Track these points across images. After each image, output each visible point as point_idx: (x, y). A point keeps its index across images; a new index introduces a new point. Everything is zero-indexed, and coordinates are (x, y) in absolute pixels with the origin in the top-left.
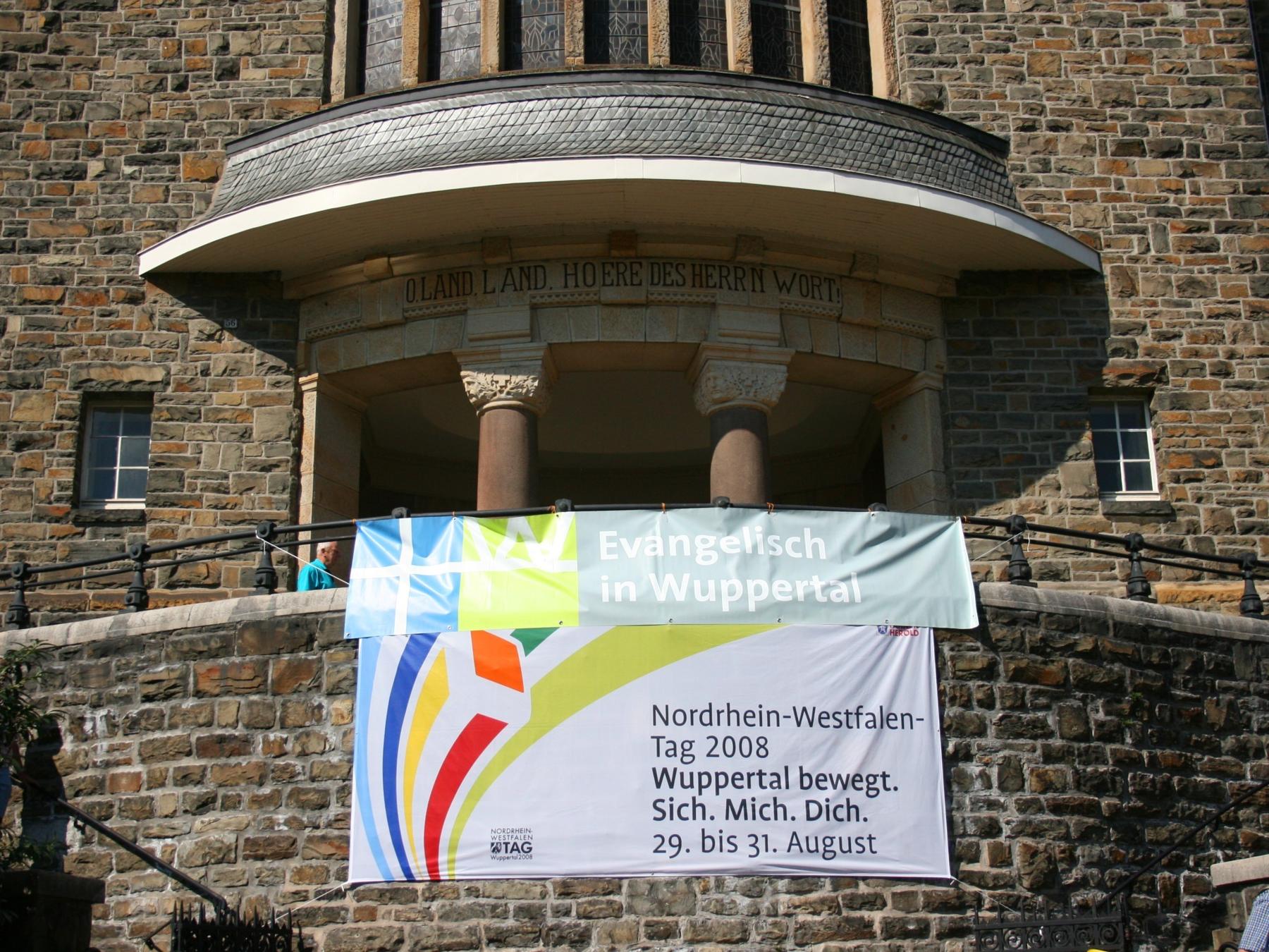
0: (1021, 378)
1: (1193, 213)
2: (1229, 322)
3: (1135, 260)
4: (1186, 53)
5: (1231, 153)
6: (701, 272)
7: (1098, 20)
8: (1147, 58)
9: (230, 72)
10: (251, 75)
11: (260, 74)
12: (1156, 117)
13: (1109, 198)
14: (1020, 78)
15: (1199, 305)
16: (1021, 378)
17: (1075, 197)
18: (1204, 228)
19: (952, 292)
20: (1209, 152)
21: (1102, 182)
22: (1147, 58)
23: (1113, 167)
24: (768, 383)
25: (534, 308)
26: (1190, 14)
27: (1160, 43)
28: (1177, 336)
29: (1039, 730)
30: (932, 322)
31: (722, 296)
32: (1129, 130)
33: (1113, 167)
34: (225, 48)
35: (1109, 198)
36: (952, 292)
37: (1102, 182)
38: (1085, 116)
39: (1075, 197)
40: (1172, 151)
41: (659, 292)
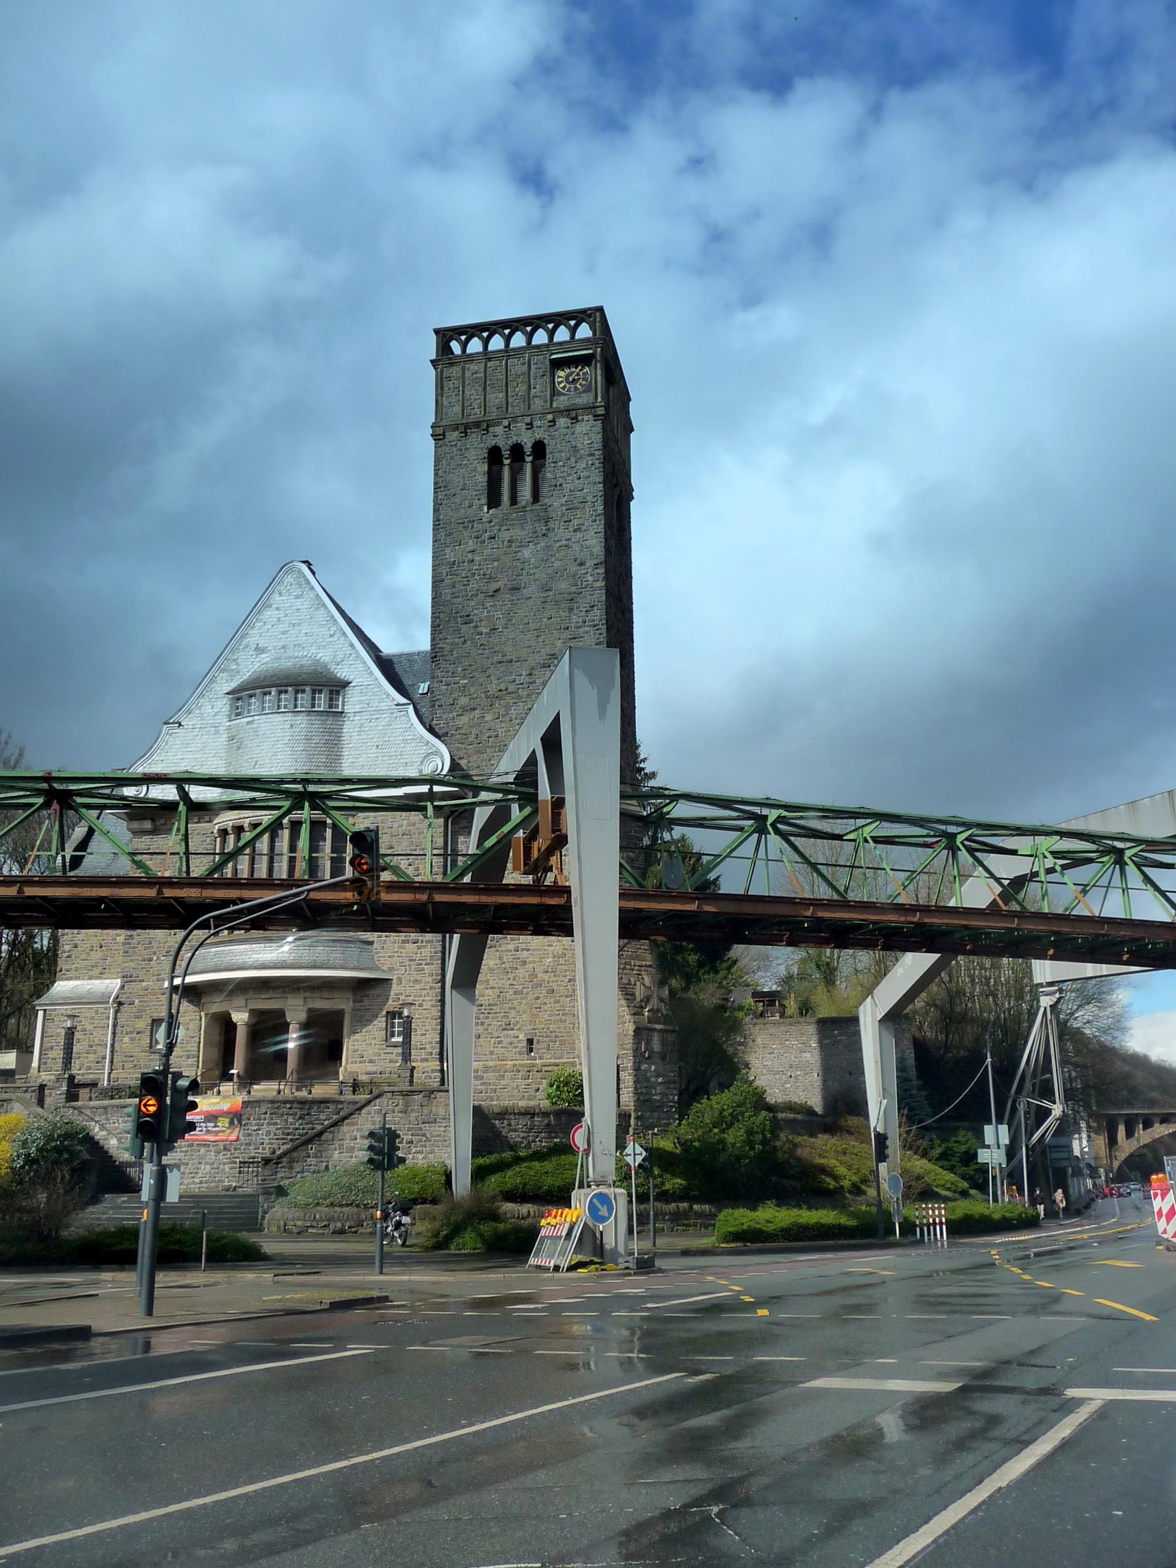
15: (417, 987)
23: (400, 947)
24: (303, 1016)
29: (276, 1124)
31: (290, 995)
33: (400, 947)
41: (274, 995)
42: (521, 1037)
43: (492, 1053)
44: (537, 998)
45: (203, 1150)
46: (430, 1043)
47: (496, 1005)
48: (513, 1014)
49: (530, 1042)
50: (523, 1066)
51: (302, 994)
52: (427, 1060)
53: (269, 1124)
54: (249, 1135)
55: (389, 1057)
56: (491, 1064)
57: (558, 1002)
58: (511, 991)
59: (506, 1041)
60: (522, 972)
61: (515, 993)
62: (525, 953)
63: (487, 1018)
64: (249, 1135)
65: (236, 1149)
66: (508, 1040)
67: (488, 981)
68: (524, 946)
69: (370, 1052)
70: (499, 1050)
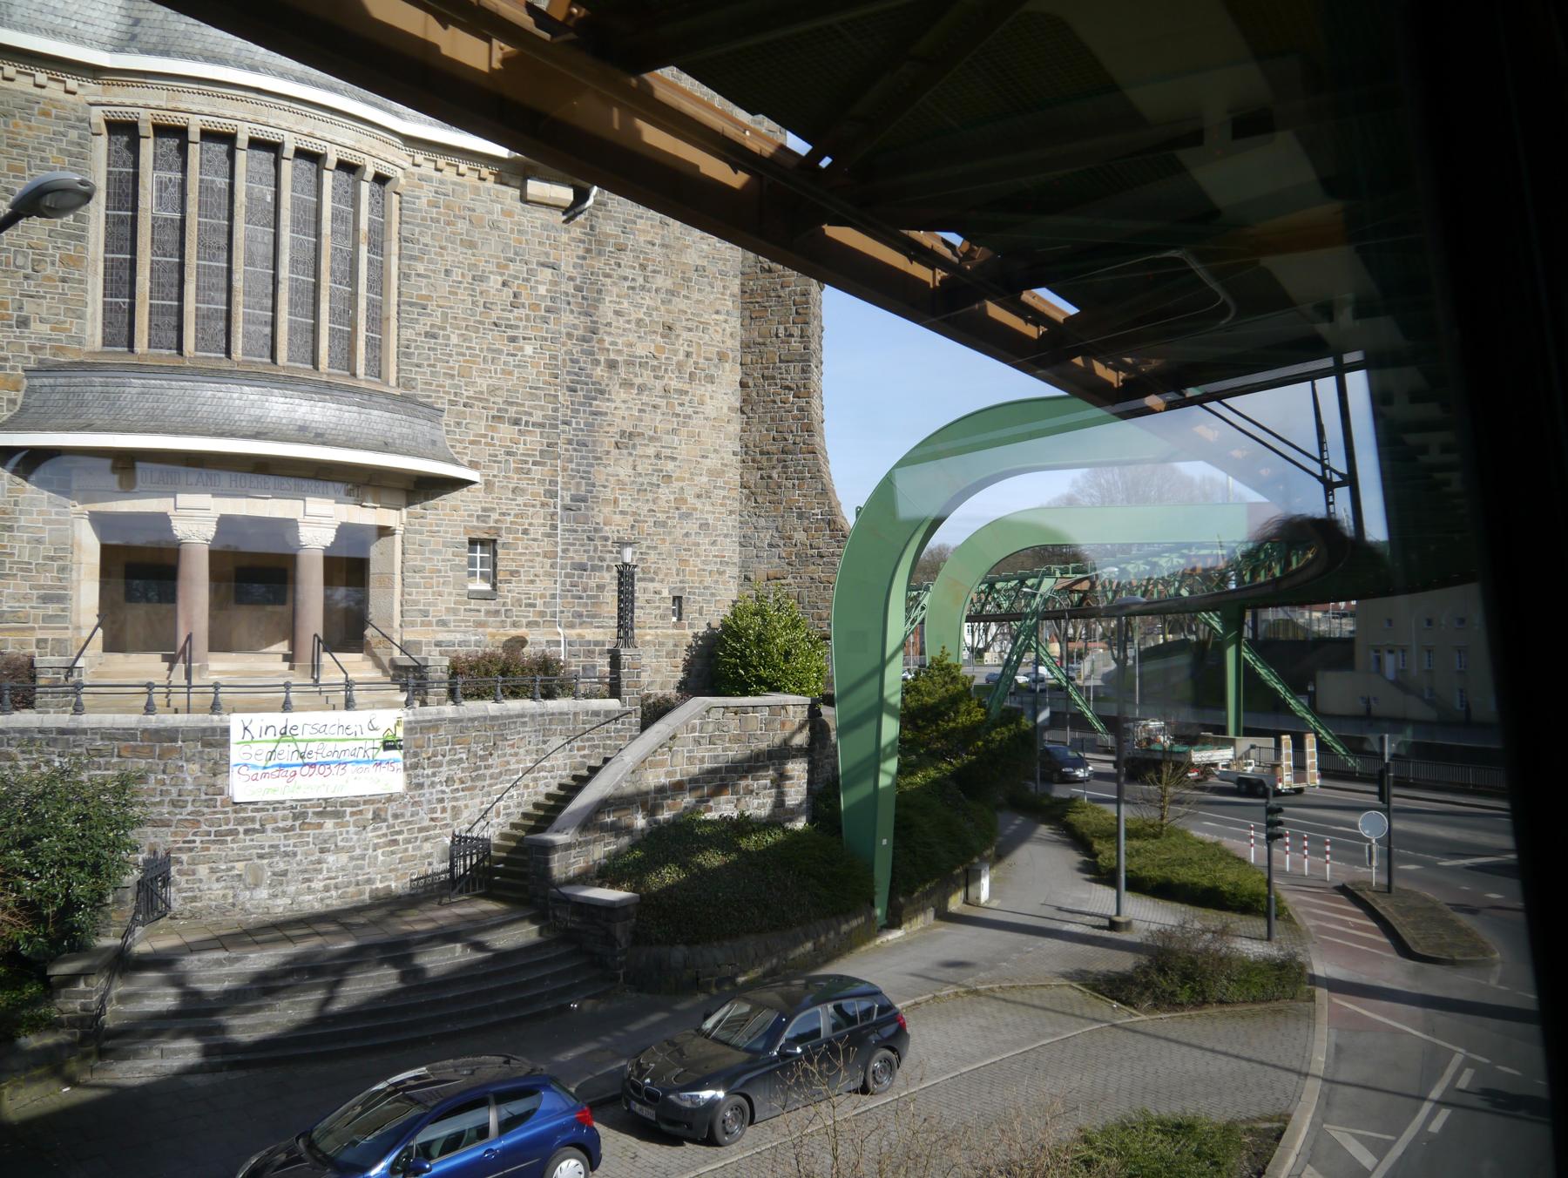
4: (531, 373)
5: (542, 425)
7: (494, 351)
8: (511, 373)
9: (23, 323)
10: (35, 326)
11: (45, 328)
12: (511, 404)
13: (487, 444)
14: (452, 376)
15: (520, 500)
17: (472, 443)
18: (526, 462)
19: (411, 487)
20: (534, 425)
21: (485, 436)
22: (511, 373)
27: (519, 366)
32: (499, 410)
33: (493, 429)
34: (21, 308)
35: (487, 444)
36: (411, 487)
37: (485, 436)
38: (481, 400)
39: (472, 443)
40: (516, 422)
42: (665, 593)
44: (687, 535)
45: (329, 824)
49: (677, 600)
50: (668, 636)
52: (536, 624)
53: (451, 762)
54: (421, 786)
55: (473, 617)
57: (714, 543)
60: (665, 494)
62: (670, 466)
64: (421, 786)
65: (396, 816)
66: (647, 596)
67: (616, 501)
68: (668, 452)
69: (442, 607)
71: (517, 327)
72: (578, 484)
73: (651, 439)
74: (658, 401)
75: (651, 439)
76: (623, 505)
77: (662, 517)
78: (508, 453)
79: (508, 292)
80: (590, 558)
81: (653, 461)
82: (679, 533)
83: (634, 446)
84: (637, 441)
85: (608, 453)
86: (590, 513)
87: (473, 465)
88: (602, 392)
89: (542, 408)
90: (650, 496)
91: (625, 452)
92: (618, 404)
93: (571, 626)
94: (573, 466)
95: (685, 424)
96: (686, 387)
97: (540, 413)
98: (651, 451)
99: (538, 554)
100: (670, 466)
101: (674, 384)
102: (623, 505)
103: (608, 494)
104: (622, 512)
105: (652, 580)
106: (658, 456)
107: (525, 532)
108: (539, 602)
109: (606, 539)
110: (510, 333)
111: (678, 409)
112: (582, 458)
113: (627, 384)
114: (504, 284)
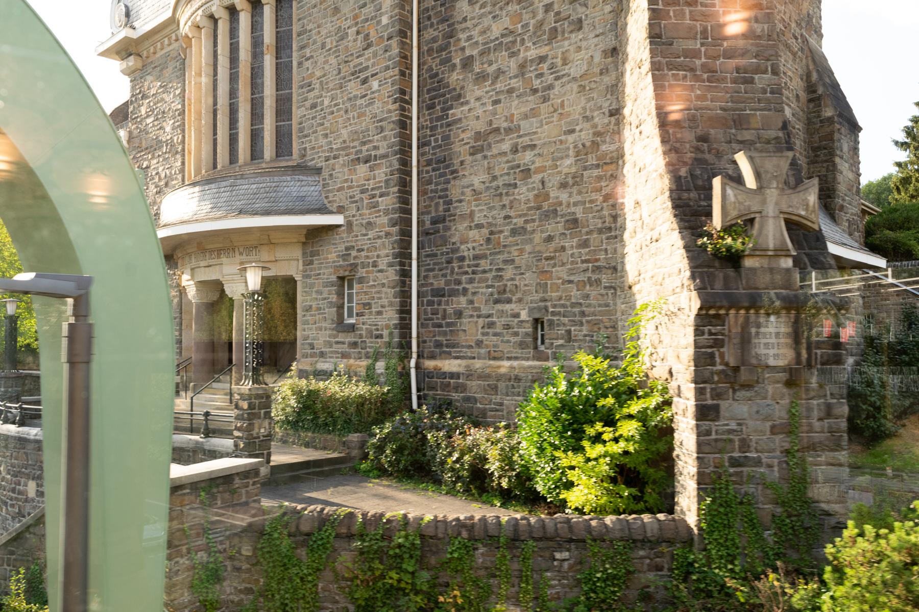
0: (319, 274)
1: (372, 189)
2: (379, 241)
3: (353, 216)
6: (219, 252)
7: (350, 99)
16: (319, 274)
19: (304, 240)
25: (192, 269)
26: (380, 86)
28: (363, 250)
30: (297, 252)
31: (224, 260)
32: (357, 153)
36: (304, 240)
38: (343, 149)
41: (212, 262)
42: (524, 315)
43: (479, 344)
44: (550, 239)
46: (387, 327)
47: (484, 257)
48: (509, 272)
51: (238, 258)
56: (478, 364)
58: (507, 229)
59: (500, 322)
60: (524, 193)
61: (514, 232)
63: (471, 281)
66: (504, 320)
67: (472, 214)
68: (526, 140)
70: (490, 340)
71: (367, 68)
72: (437, 204)
73: (509, 131)
74: (514, 83)
75: (509, 131)
76: (479, 218)
77: (520, 222)
78: (362, 192)
79: (361, 37)
80: (448, 283)
81: (510, 157)
82: (538, 238)
83: (489, 145)
84: (491, 139)
85: (462, 163)
86: (448, 234)
87: (340, 210)
88: (459, 96)
89: (385, 138)
90: (506, 200)
91: (479, 156)
92: (472, 105)
93: (432, 357)
94: (433, 187)
95: (545, 99)
96: (544, 51)
97: (385, 144)
98: (506, 146)
99: (383, 285)
100: (527, 157)
101: (533, 53)
102: (479, 218)
103: (464, 209)
104: (479, 226)
105: (509, 301)
106: (515, 150)
107: (375, 265)
108: (385, 333)
109: (462, 259)
110: (363, 76)
111: (537, 83)
112: (441, 176)
113: (481, 78)
114: (358, 33)
